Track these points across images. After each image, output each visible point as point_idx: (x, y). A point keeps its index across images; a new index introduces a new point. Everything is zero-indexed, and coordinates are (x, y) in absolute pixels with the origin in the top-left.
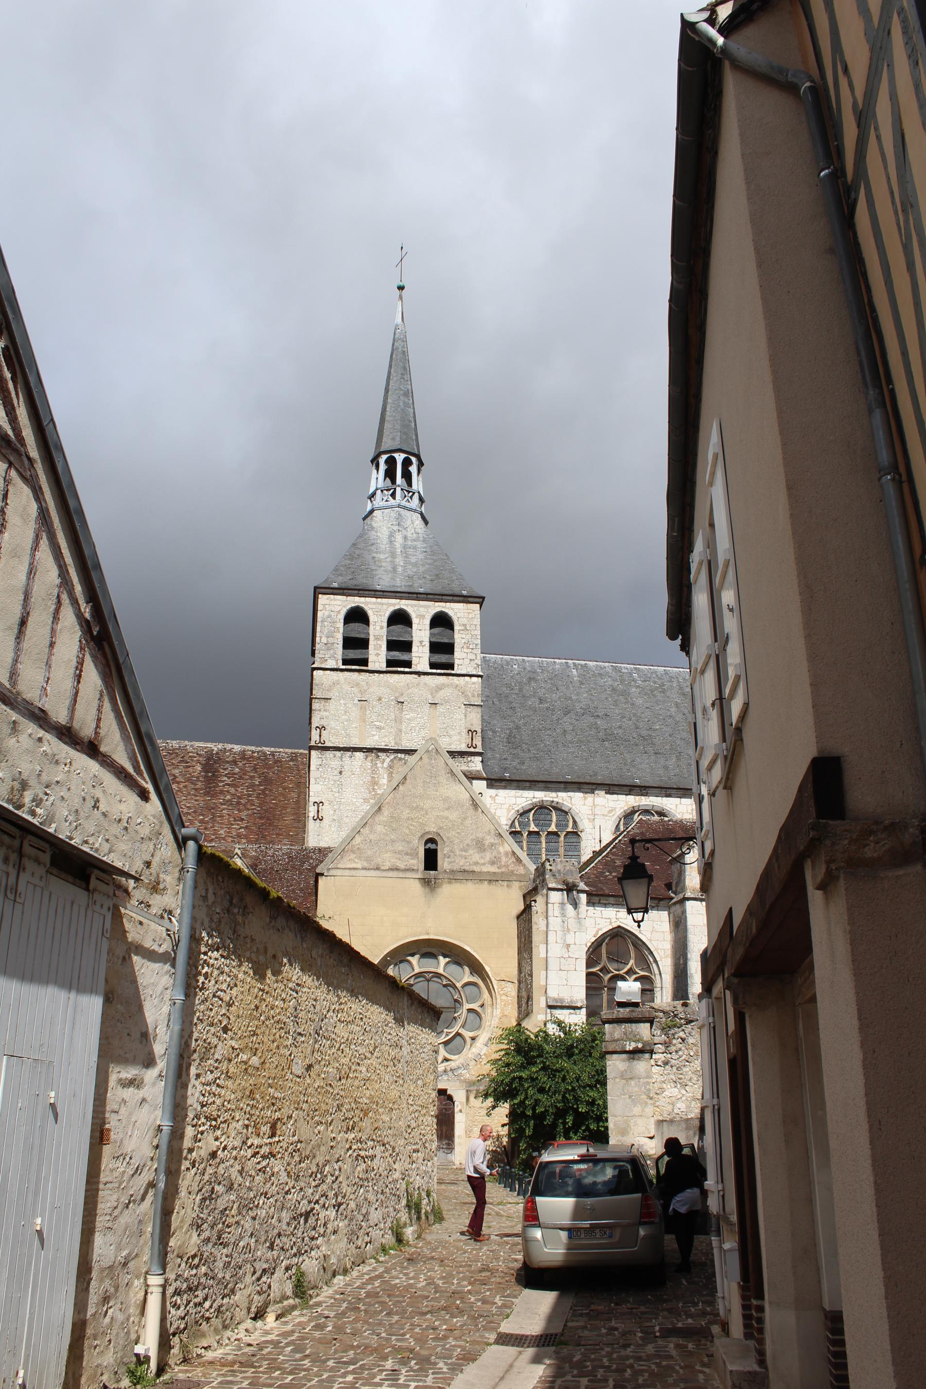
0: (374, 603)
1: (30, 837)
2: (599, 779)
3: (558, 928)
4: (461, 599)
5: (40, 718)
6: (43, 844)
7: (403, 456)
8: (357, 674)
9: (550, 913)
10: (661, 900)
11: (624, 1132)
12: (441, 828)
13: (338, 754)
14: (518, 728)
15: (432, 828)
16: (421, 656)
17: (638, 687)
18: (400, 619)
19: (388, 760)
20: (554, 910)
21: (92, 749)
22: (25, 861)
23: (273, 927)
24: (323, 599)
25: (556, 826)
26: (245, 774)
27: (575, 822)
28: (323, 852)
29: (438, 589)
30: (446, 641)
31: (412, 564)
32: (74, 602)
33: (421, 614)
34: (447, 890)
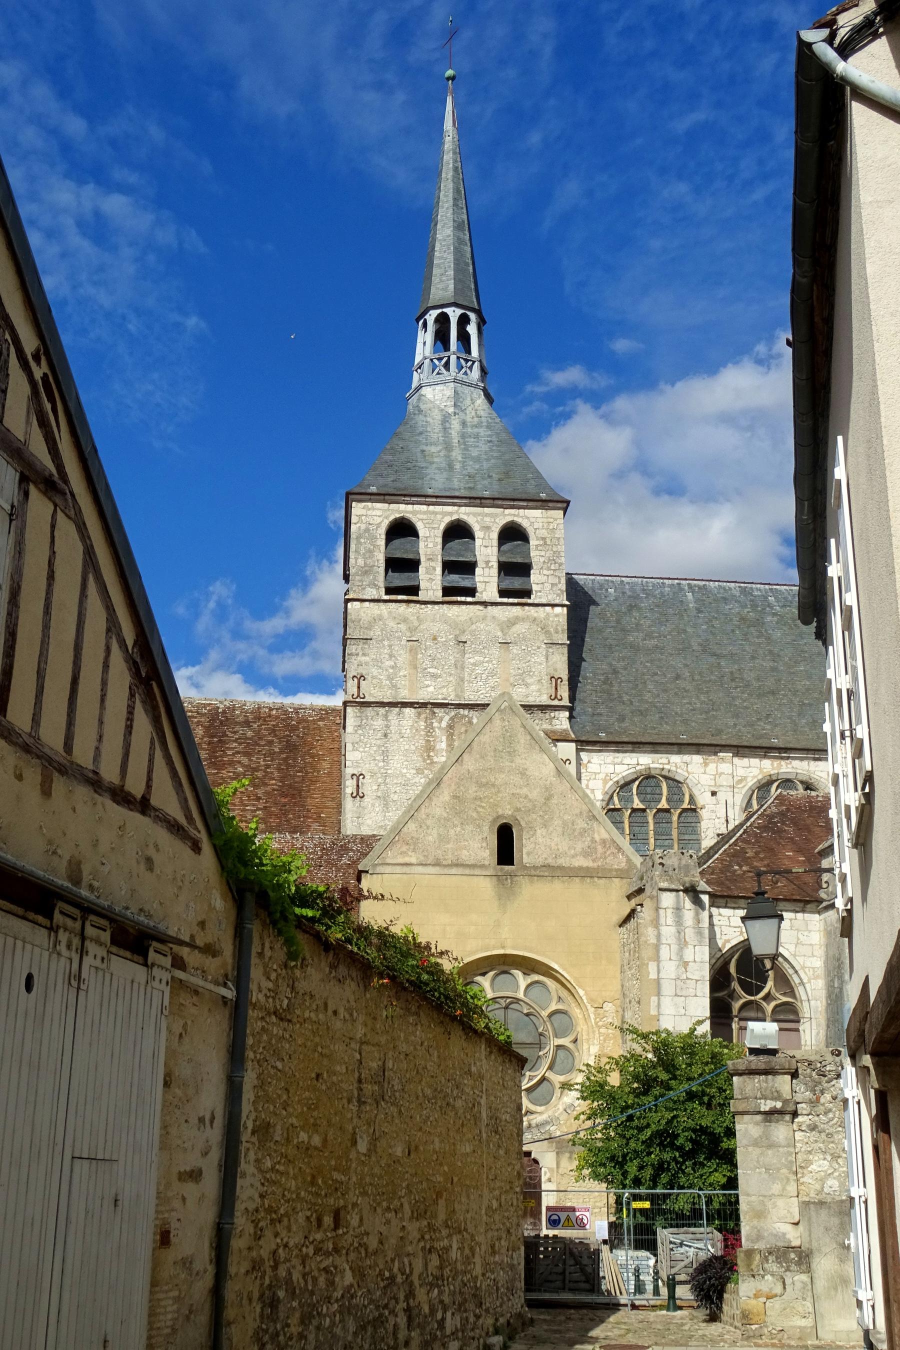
0: (425, 513)
1: (92, 917)
2: (723, 739)
3: (672, 941)
4: (539, 504)
5: (95, 782)
6: (104, 922)
7: (459, 312)
8: (404, 605)
9: (662, 921)
10: (808, 902)
11: (760, 1214)
12: (518, 810)
13: (382, 711)
14: (615, 672)
15: (506, 812)
16: (487, 580)
17: (774, 614)
18: (458, 532)
19: (447, 718)
21: (144, 806)
22: (87, 943)
23: (334, 977)
24: (357, 509)
25: (668, 800)
26: (260, 739)
27: (692, 798)
28: (367, 842)
29: (509, 492)
30: (520, 560)
31: (473, 458)
32: (122, 643)
33: (486, 524)
34: (530, 891)
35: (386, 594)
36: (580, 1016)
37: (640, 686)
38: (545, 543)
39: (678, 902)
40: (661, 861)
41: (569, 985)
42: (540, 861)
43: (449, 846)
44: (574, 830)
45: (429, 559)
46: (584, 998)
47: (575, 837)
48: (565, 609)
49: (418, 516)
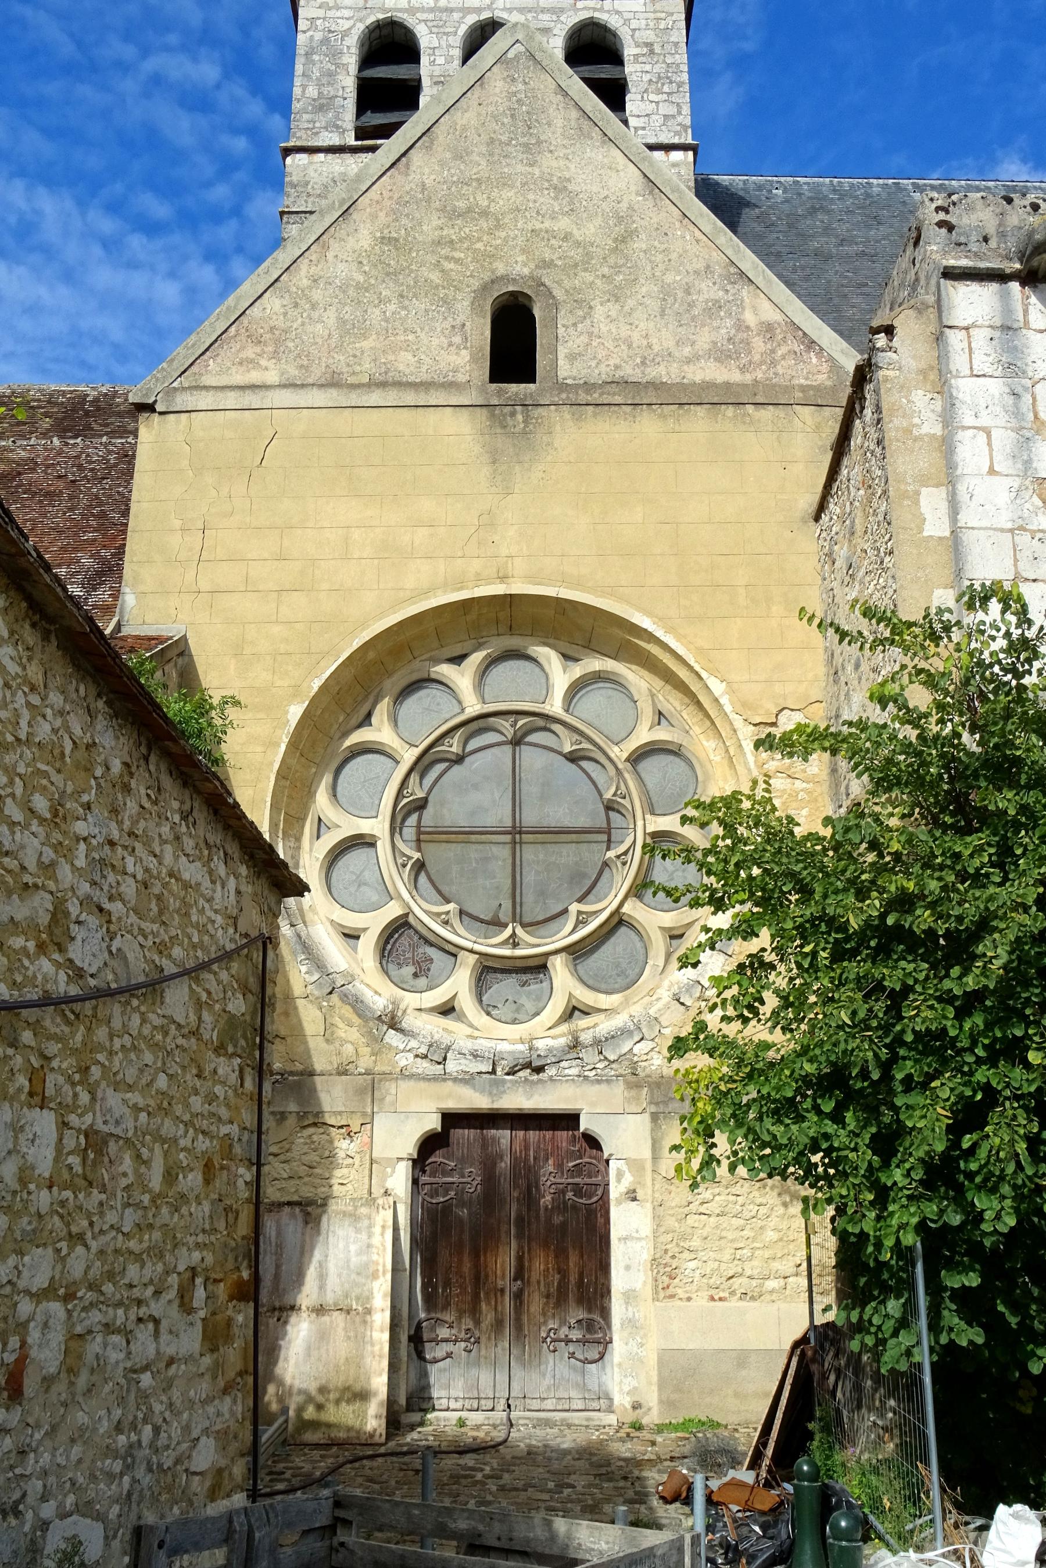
3: (996, 419)
9: (958, 361)
15: (516, 268)
20: (973, 353)
34: (571, 439)
35: (357, 139)
36: (717, 758)
37: (836, 301)
38: (652, 52)
39: (1007, 310)
40: (942, 216)
41: (683, 673)
42: (601, 372)
43: (366, 344)
44: (691, 305)
45: (436, 83)
46: (724, 700)
47: (693, 318)
48: (691, 154)
49: (418, 15)
